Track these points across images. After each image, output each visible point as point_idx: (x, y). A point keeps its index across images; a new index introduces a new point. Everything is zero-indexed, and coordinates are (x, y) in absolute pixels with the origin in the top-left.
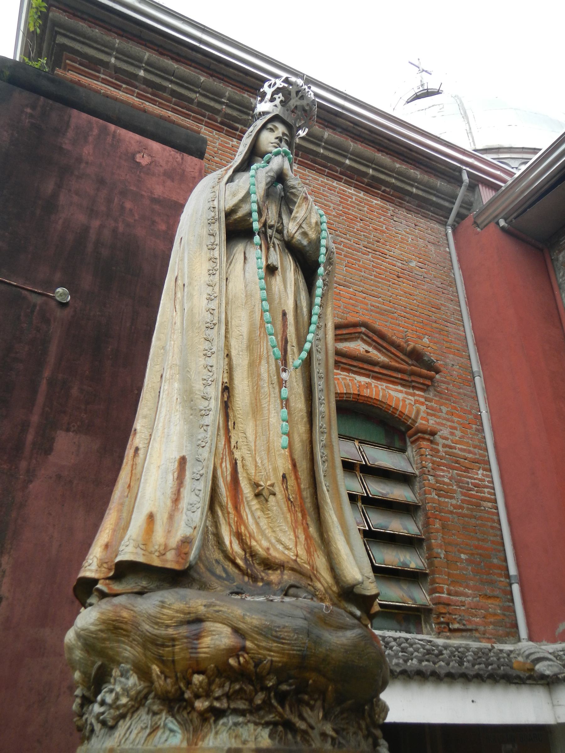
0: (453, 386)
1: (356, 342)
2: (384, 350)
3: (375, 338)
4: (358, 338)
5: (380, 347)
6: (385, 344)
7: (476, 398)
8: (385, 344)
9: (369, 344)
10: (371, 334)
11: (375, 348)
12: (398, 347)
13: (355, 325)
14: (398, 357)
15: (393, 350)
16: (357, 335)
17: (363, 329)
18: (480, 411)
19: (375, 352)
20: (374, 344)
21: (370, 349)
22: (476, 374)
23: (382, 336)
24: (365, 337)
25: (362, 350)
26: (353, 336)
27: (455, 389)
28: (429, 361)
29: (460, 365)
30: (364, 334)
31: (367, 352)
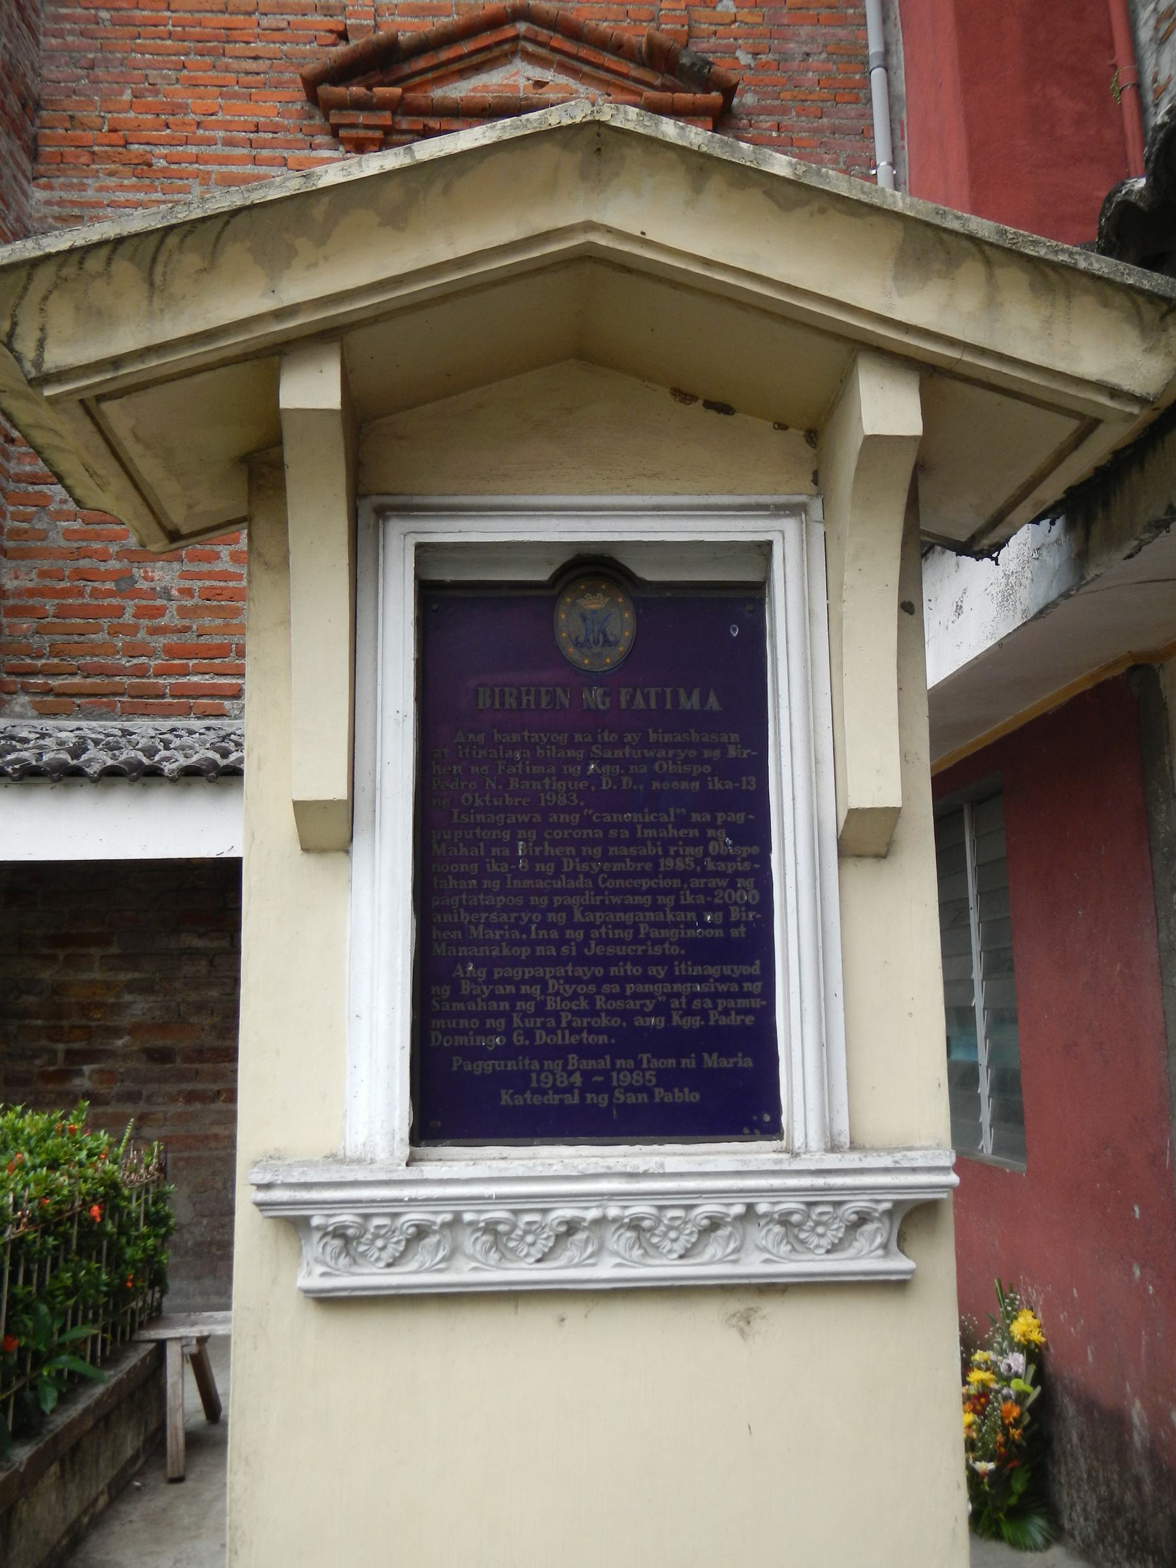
0: (798, 115)
1: (509, 67)
2: (586, 68)
3: (558, 41)
4: (513, 53)
5: (575, 63)
6: (584, 52)
7: (867, 133)
8: (584, 52)
9: (543, 62)
10: (544, 34)
11: (564, 69)
12: (618, 48)
13: (495, 22)
14: (626, 76)
15: (609, 60)
16: (506, 47)
17: (522, 27)
18: (875, 167)
19: (563, 79)
20: (558, 57)
21: (548, 75)
22: (874, 62)
23: (573, 32)
24: (530, 48)
25: (522, 82)
26: (496, 52)
27: (803, 122)
28: (693, 64)
29: (830, 49)
30: (526, 38)
31: (539, 84)
